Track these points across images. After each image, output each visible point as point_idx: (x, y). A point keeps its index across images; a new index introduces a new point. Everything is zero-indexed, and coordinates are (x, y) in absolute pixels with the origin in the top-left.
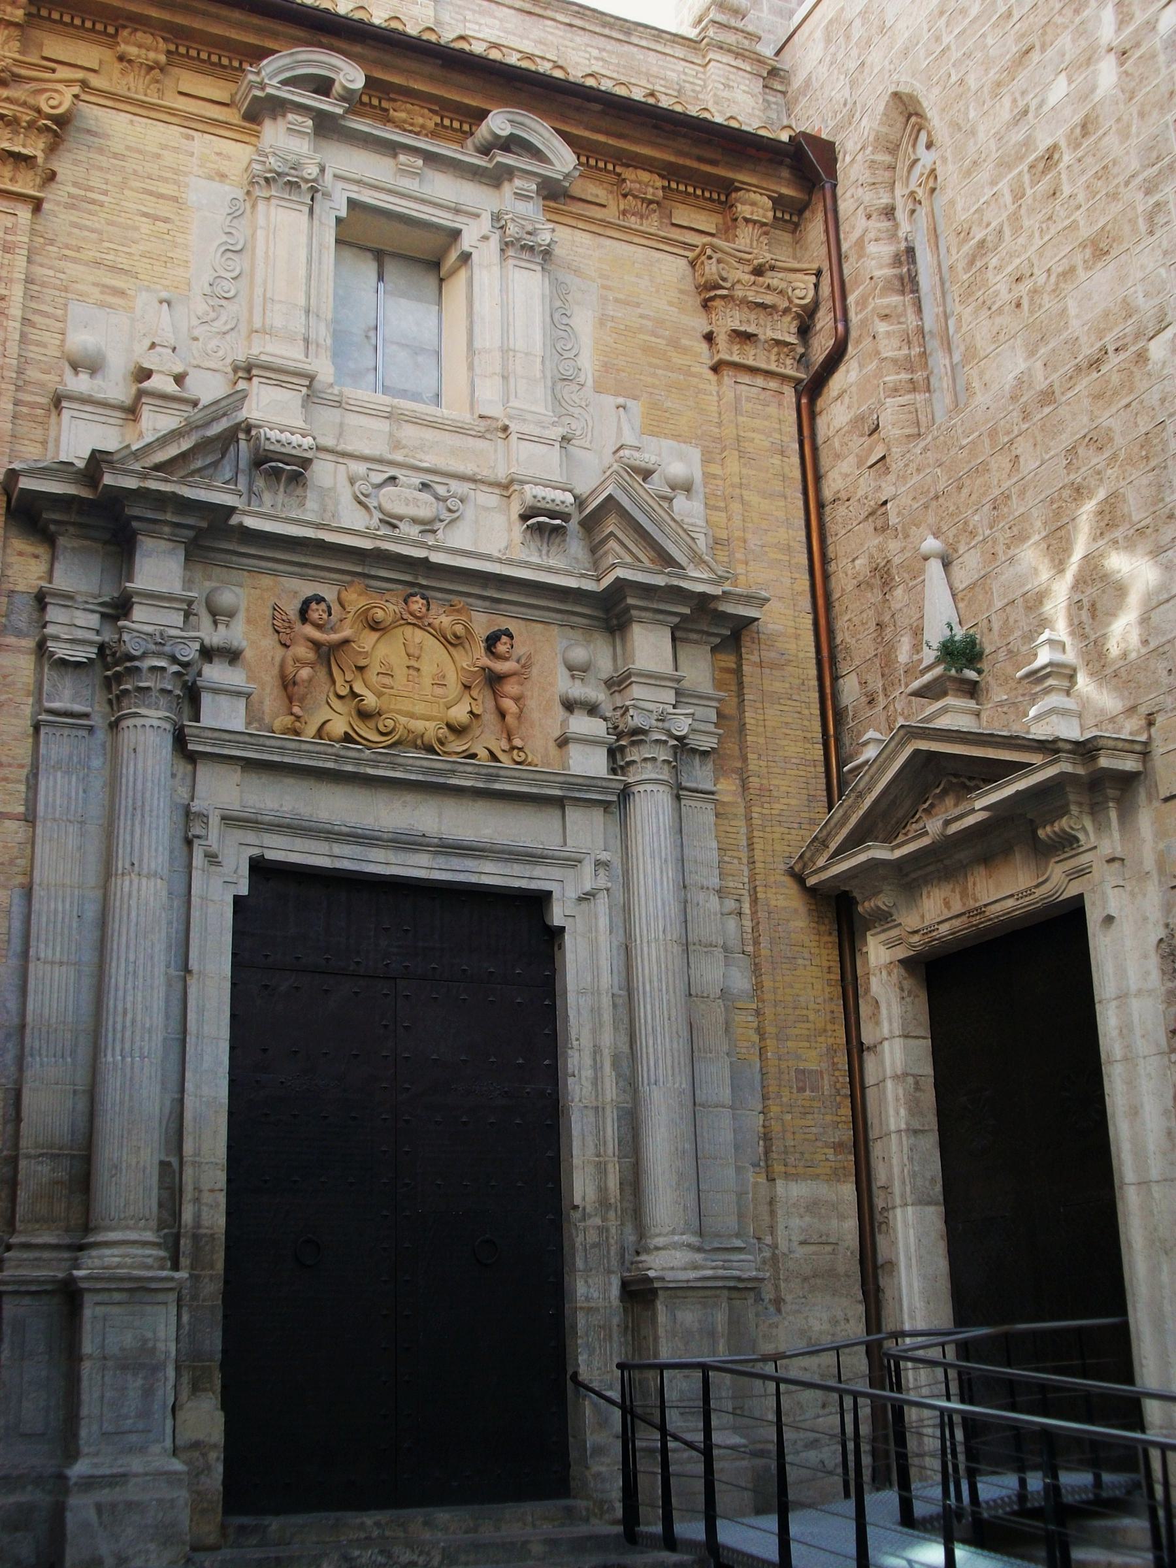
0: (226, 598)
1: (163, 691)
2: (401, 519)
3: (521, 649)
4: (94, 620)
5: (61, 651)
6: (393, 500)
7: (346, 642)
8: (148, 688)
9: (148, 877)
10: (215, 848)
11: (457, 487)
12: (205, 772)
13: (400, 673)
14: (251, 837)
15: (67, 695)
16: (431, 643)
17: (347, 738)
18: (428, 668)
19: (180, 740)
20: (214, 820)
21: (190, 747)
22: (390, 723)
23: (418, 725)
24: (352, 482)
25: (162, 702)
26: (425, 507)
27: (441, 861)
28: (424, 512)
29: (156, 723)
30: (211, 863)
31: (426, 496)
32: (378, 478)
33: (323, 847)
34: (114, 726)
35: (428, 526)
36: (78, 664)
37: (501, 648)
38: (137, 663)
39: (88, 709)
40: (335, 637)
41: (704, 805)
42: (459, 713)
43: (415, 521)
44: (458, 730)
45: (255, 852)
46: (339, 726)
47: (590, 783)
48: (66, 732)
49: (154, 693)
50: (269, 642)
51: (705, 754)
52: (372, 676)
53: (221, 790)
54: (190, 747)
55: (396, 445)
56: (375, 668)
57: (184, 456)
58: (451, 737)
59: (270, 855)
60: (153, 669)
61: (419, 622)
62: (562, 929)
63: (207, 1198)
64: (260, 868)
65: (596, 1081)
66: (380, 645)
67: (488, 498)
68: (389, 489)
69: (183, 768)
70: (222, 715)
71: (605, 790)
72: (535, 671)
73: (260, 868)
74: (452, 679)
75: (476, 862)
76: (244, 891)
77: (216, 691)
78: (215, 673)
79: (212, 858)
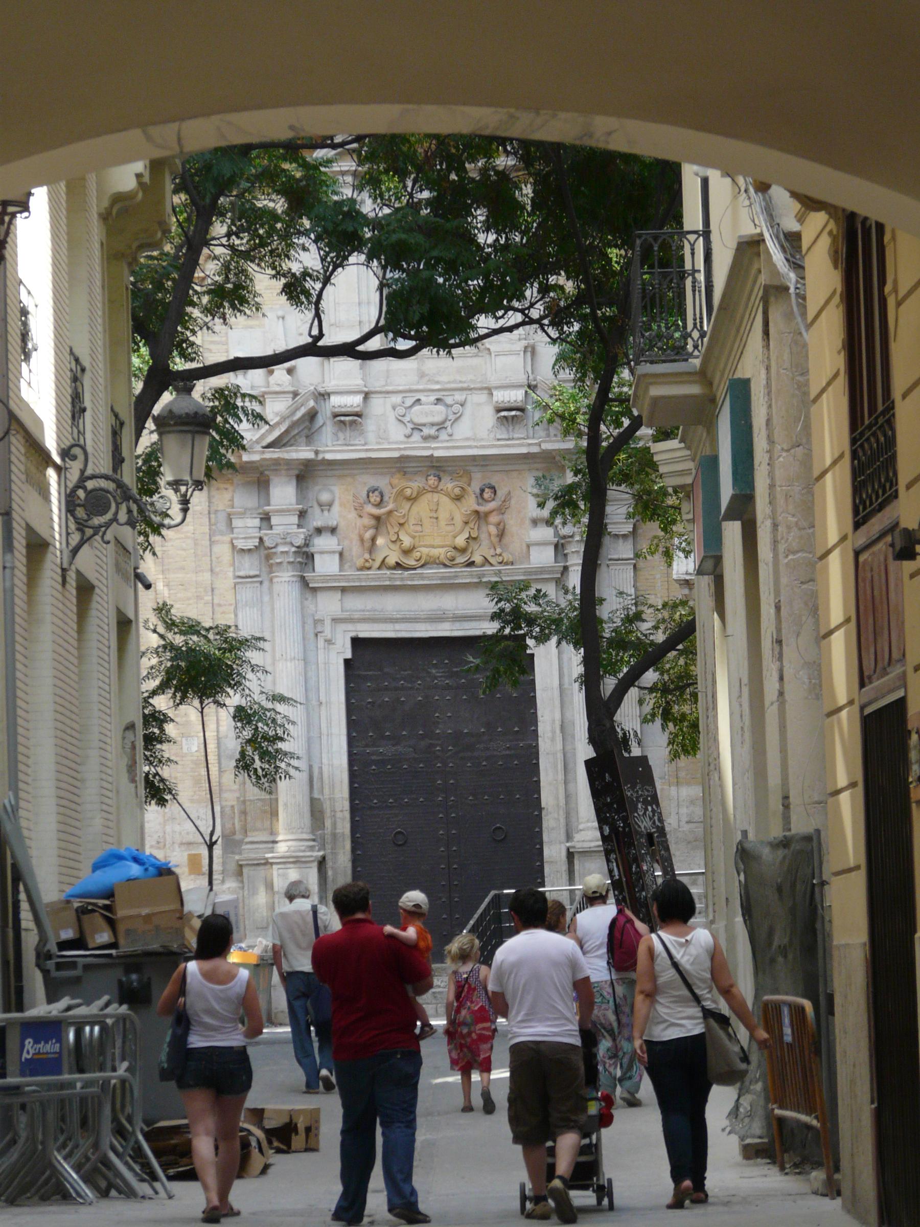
0: (325, 497)
1: (289, 562)
2: (424, 425)
3: (501, 493)
4: (257, 522)
5: (240, 544)
6: (419, 415)
7: (390, 513)
8: (281, 563)
9: (291, 660)
10: (329, 637)
11: (459, 397)
12: (322, 598)
13: (427, 522)
14: (350, 627)
15: (249, 566)
16: (445, 500)
17: (398, 566)
18: (443, 515)
19: (304, 582)
20: (328, 622)
21: (311, 585)
22: (418, 554)
23: (435, 552)
24: (394, 408)
25: (290, 567)
26: (438, 413)
27: (457, 625)
28: (438, 419)
29: (287, 579)
30: (329, 644)
31: (440, 408)
32: (409, 402)
33: (390, 626)
34: (271, 580)
35: (441, 426)
36: (250, 550)
37: (487, 494)
38: (274, 550)
39: (258, 573)
40: (383, 511)
41: (625, 567)
42: (460, 541)
43: (433, 425)
44: (463, 551)
45: (353, 634)
46: (392, 561)
47: (542, 570)
48: (248, 585)
49: (285, 564)
50: (353, 515)
51: (625, 536)
52: (410, 527)
53: (329, 605)
54: (311, 585)
55: (422, 375)
56: (412, 521)
57: (287, 432)
58: (458, 554)
59: (361, 635)
60: (282, 552)
61: (435, 490)
62: (532, 655)
63: (339, 815)
64: (357, 642)
65: (553, 739)
66: (413, 507)
67: (482, 397)
68: (417, 408)
69: (309, 595)
70: (326, 566)
71: (552, 572)
72: (513, 502)
73: (357, 642)
74: (459, 520)
75: (478, 623)
76: (349, 655)
77: (322, 553)
78: (323, 543)
79: (329, 642)
